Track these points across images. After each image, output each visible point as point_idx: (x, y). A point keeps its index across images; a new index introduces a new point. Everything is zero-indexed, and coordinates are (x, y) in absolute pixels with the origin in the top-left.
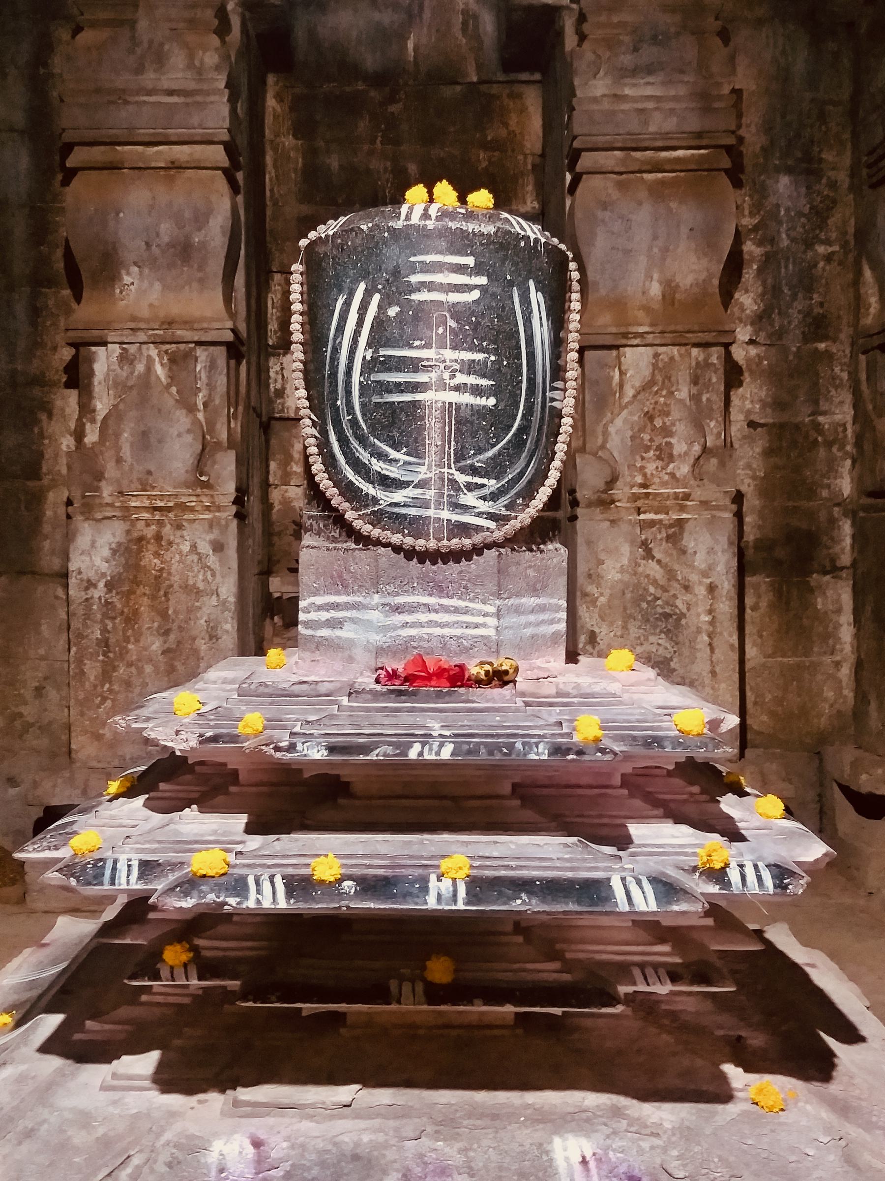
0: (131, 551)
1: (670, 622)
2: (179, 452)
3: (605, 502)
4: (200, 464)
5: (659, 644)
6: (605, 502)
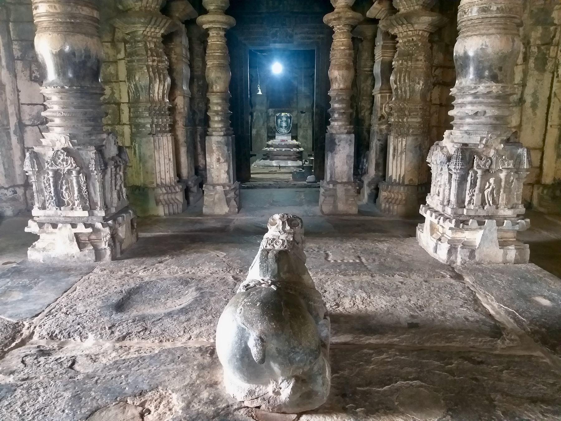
0: (257, 132)
1: (306, 138)
2: (261, 122)
3: (300, 127)
4: (263, 124)
5: (305, 140)
6: (300, 127)
